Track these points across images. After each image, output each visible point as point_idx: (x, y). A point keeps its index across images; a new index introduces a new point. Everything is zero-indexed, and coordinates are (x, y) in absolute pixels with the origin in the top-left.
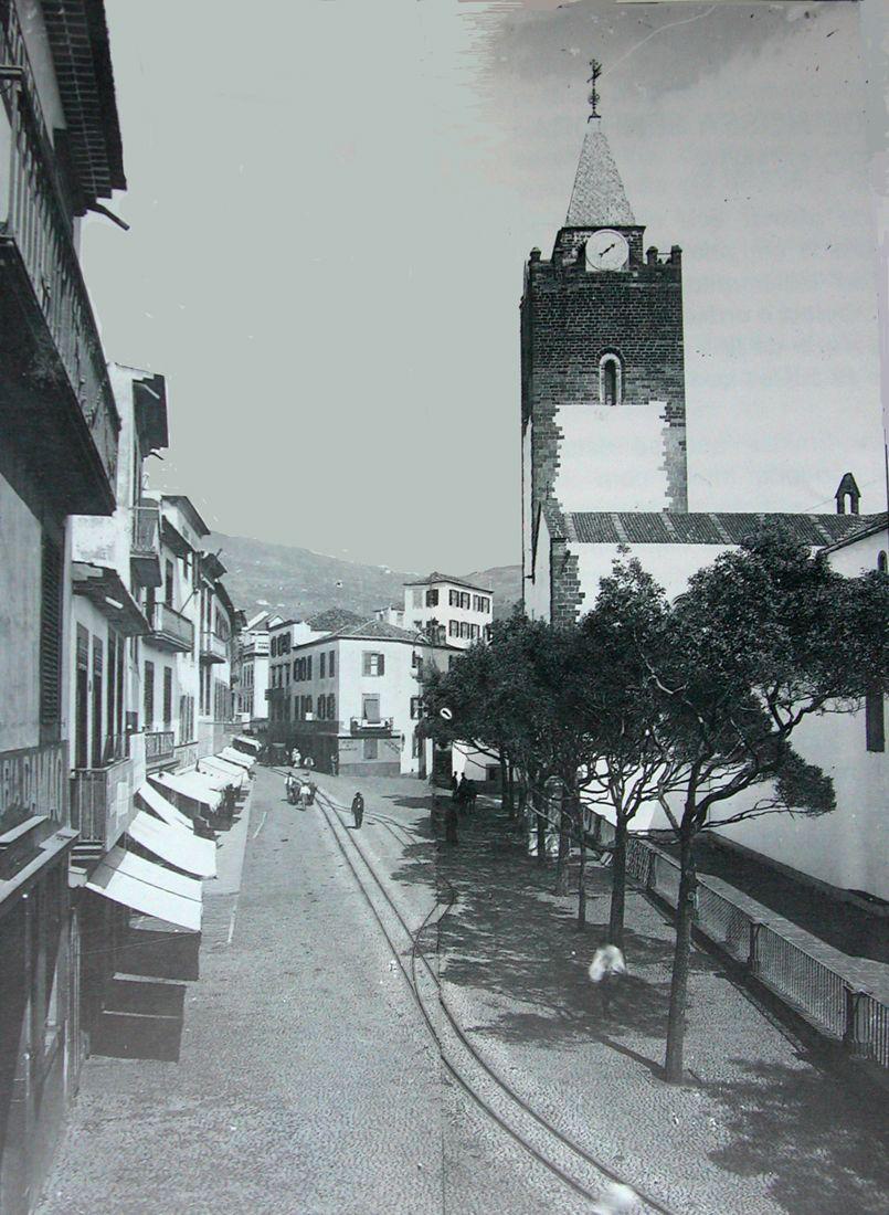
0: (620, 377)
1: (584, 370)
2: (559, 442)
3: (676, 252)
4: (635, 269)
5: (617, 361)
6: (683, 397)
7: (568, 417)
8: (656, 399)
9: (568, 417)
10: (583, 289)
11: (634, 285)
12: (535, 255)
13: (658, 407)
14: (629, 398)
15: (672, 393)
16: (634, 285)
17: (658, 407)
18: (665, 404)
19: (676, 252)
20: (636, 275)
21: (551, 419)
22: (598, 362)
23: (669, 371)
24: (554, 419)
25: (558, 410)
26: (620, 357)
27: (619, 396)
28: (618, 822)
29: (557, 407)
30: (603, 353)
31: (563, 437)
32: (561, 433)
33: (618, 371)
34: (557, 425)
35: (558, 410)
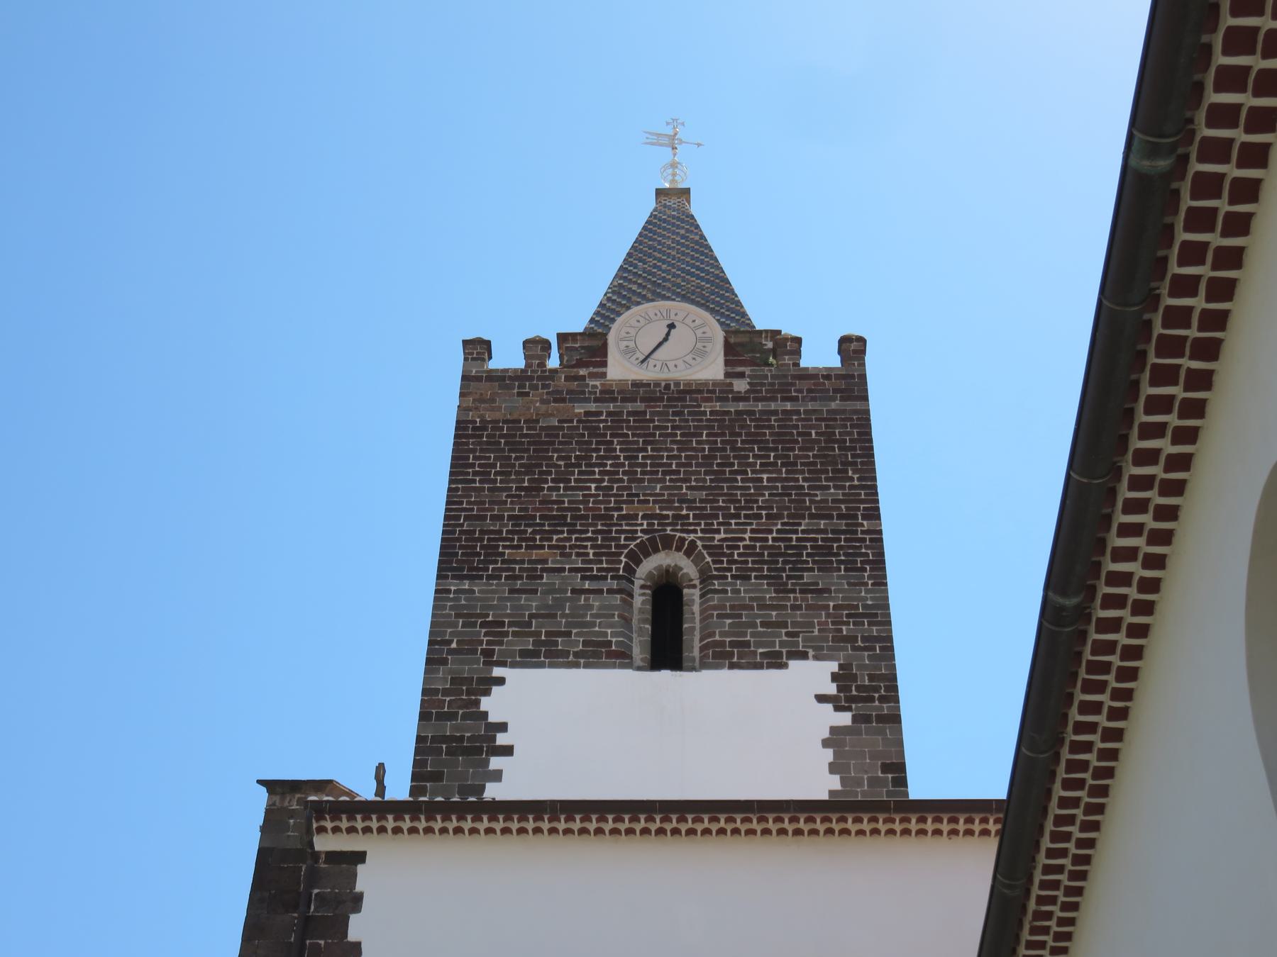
0: (696, 608)
1: (587, 585)
2: (495, 763)
3: (852, 348)
5: (688, 568)
6: (888, 650)
8: (803, 656)
10: (600, 413)
11: (742, 406)
12: (477, 349)
13: (816, 675)
15: (851, 639)
16: (742, 406)
17: (816, 675)
18: (833, 666)
19: (852, 348)
21: (478, 703)
22: (630, 571)
23: (838, 580)
24: (486, 704)
25: (501, 681)
26: (698, 560)
27: (694, 646)
29: (497, 672)
30: (648, 549)
31: (508, 751)
32: (501, 739)
33: (693, 595)
34: (492, 719)
35: (501, 681)
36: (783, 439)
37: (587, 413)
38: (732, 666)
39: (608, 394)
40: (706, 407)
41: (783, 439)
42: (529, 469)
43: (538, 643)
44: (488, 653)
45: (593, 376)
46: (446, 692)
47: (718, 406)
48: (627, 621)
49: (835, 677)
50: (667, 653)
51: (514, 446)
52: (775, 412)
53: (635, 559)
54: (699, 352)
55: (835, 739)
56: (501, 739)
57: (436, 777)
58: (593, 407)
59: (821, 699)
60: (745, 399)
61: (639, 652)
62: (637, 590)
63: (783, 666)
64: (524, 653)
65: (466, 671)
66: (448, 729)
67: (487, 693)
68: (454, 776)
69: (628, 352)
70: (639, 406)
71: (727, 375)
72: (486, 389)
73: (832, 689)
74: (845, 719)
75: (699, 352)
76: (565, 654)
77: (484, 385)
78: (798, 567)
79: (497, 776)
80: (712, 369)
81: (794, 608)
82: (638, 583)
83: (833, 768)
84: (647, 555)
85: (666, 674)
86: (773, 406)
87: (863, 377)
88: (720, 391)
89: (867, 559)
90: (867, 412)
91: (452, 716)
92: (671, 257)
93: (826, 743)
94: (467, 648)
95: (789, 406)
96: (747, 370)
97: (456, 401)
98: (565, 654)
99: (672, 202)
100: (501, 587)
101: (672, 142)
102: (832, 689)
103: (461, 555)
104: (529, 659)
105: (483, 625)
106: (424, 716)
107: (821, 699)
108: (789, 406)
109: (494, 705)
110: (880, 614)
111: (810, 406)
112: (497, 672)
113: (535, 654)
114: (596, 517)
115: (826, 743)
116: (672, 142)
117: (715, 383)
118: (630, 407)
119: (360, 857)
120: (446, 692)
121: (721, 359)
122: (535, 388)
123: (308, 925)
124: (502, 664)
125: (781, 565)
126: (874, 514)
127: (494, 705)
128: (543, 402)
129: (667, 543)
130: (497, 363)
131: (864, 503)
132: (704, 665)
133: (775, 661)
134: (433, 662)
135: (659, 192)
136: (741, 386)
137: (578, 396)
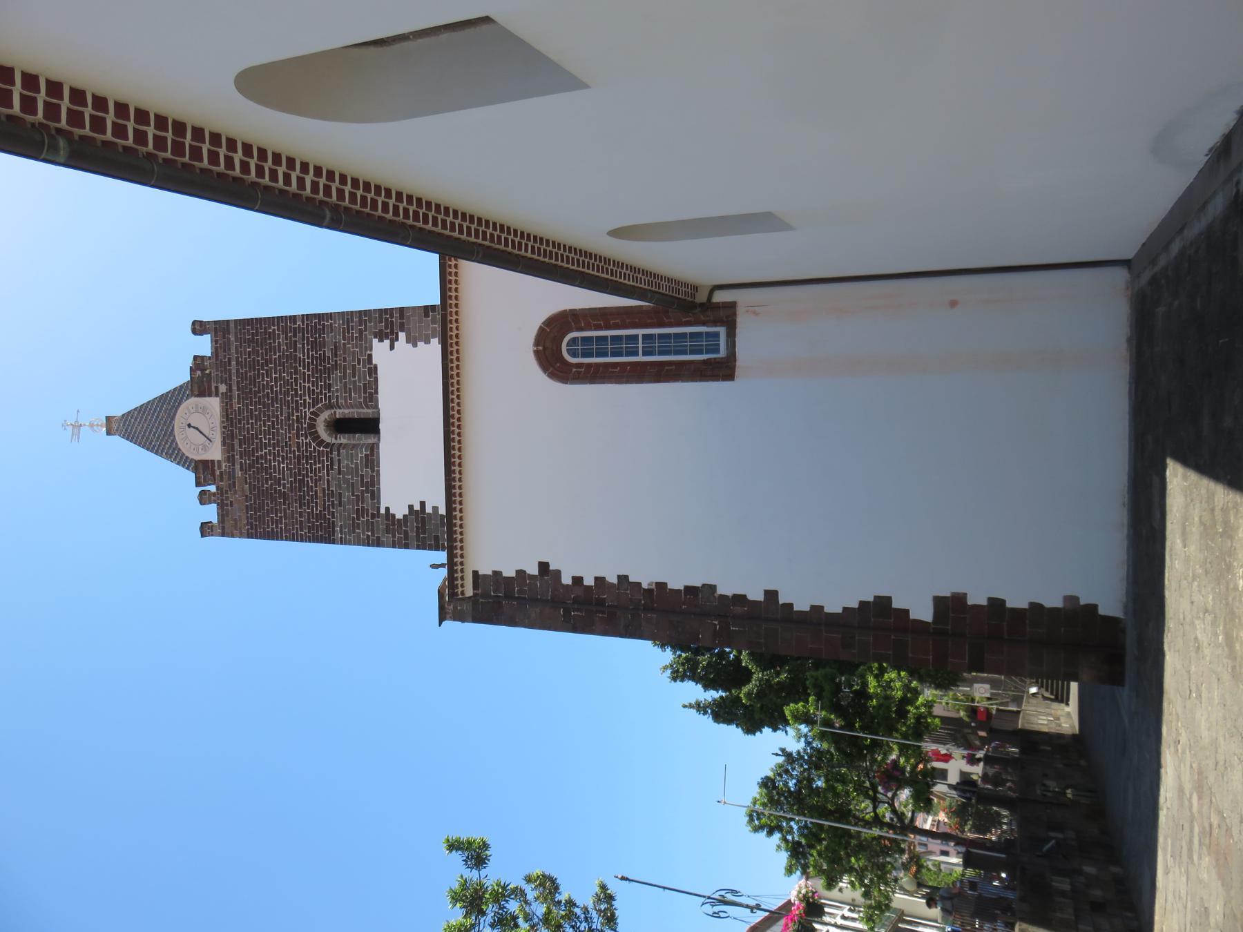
0: (346, 411)
2: (429, 510)
3: (199, 328)
4: (217, 388)
5: (325, 415)
8: (370, 356)
11: (235, 388)
13: (380, 350)
14: (371, 397)
15: (361, 332)
16: (235, 388)
17: (380, 350)
18: (375, 341)
19: (199, 328)
20: (223, 388)
22: (327, 445)
23: (329, 338)
24: (399, 516)
25: (387, 509)
27: (367, 412)
28: (1164, 468)
29: (383, 511)
30: (315, 436)
31: (423, 504)
32: (417, 507)
33: (339, 413)
35: (387, 509)
36: (252, 366)
37: (241, 469)
38: (376, 392)
39: (230, 459)
40: (236, 407)
41: (252, 366)
42: (273, 499)
43: (367, 491)
44: (373, 516)
45: (220, 467)
46: (394, 536)
48: (354, 446)
49: (381, 340)
50: (370, 426)
51: (261, 507)
52: (238, 370)
53: (321, 443)
54: (204, 411)
55: (413, 341)
56: (417, 507)
57: (437, 539)
58: (237, 467)
59: (392, 347)
60: (230, 386)
61: (371, 440)
62: (338, 441)
63: (376, 367)
64: (373, 497)
65: (382, 527)
66: (412, 534)
67: (394, 516)
68: (435, 530)
69: (205, 449)
70: (236, 442)
71: (217, 395)
72: (229, 523)
73: (387, 342)
74: (402, 336)
75: (204, 411)
76: (372, 477)
77: (227, 525)
78: (323, 359)
79: (435, 509)
80: (214, 404)
81: (345, 360)
82: (334, 441)
83: (427, 342)
84: (319, 437)
85: (381, 426)
86: (234, 371)
87: (216, 322)
88: (227, 399)
89: (319, 321)
90: (236, 321)
91: (406, 533)
92: (149, 426)
93: (415, 345)
94: (371, 526)
95: (234, 363)
96: (214, 385)
97: (237, 540)
98: (372, 477)
99: (115, 426)
100: (338, 511)
101: (77, 427)
102: (387, 342)
103: (323, 532)
104: (375, 495)
105: (358, 519)
106: (406, 546)
107: (392, 347)
108: (234, 363)
109: (400, 512)
110: (347, 317)
111: (233, 351)
112: (383, 511)
113: (373, 493)
114: (299, 463)
115: (415, 345)
116: (77, 427)
117: (222, 402)
118: (237, 447)
119: (475, 573)
120: (394, 536)
121: (207, 399)
122: (227, 498)
123: (509, 596)
124: (379, 508)
125: (322, 368)
126: (293, 318)
127: (400, 512)
128: (235, 492)
129: (312, 426)
130: (214, 519)
131: (288, 324)
132: (377, 407)
133: (373, 370)
134: (378, 544)
135: (109, 433)
136: (223, 388)
137: (231, 475)
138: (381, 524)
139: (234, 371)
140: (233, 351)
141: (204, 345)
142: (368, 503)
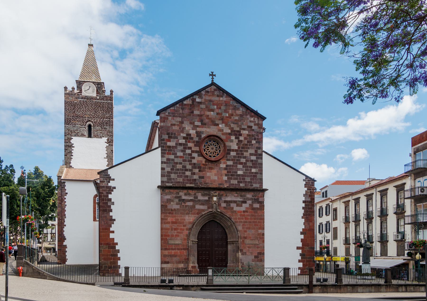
3: (112, 92)
7: (75, 140)
9: (75, 140)
11: (98, 101)
16: (98, 101)
19: (112, 92)
29: (72, 137)
30: (87, 122)
36: (103, 107)
41: (103, 107)
47: (95, 101)
53: (86, 123)
61: (86, 133)
86: (102, 101)
88: (96, 99)
109: (72, 141)
112: (72, 137)
138: (69, 136)
139: (102, 101)
140: (106, 101)
141: (108, 93)
142: (74, 134)
